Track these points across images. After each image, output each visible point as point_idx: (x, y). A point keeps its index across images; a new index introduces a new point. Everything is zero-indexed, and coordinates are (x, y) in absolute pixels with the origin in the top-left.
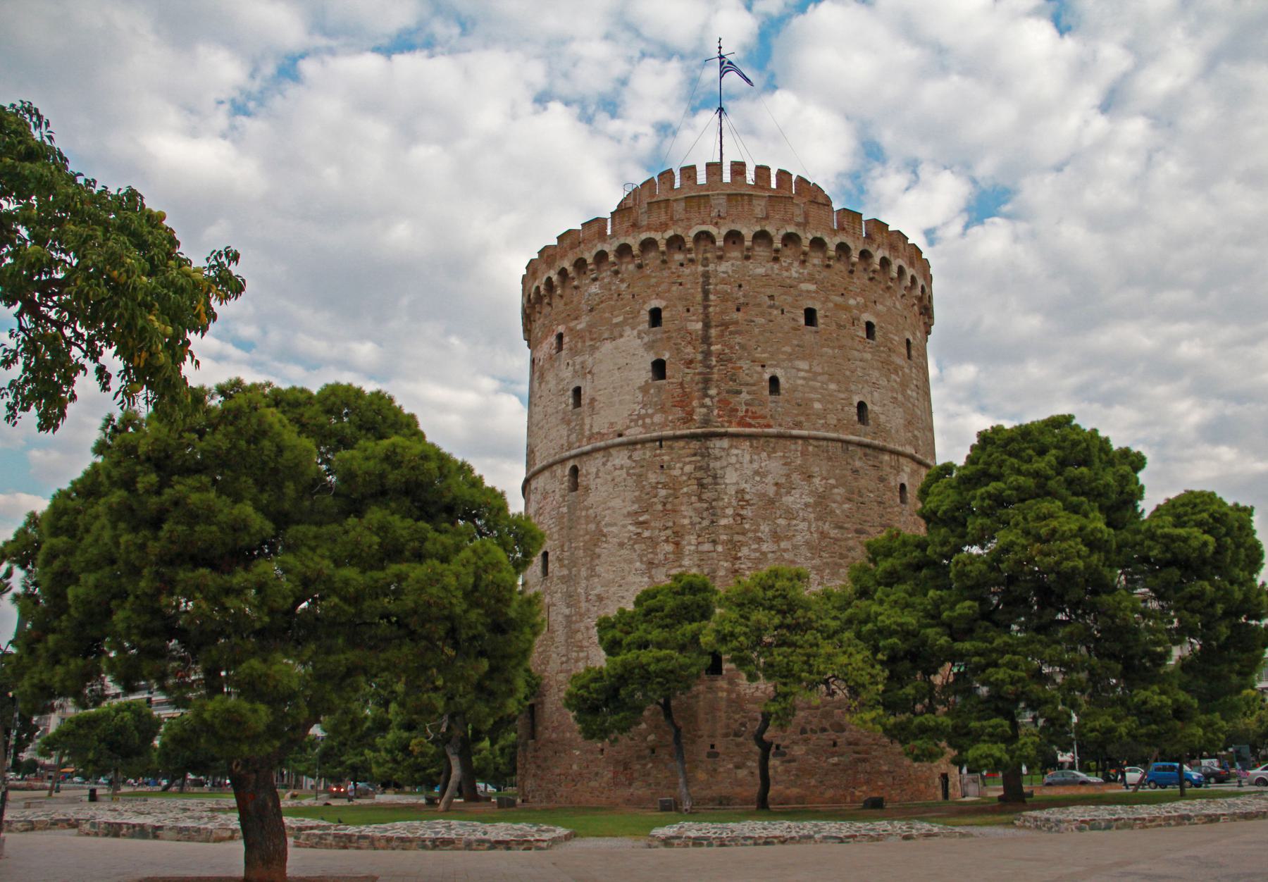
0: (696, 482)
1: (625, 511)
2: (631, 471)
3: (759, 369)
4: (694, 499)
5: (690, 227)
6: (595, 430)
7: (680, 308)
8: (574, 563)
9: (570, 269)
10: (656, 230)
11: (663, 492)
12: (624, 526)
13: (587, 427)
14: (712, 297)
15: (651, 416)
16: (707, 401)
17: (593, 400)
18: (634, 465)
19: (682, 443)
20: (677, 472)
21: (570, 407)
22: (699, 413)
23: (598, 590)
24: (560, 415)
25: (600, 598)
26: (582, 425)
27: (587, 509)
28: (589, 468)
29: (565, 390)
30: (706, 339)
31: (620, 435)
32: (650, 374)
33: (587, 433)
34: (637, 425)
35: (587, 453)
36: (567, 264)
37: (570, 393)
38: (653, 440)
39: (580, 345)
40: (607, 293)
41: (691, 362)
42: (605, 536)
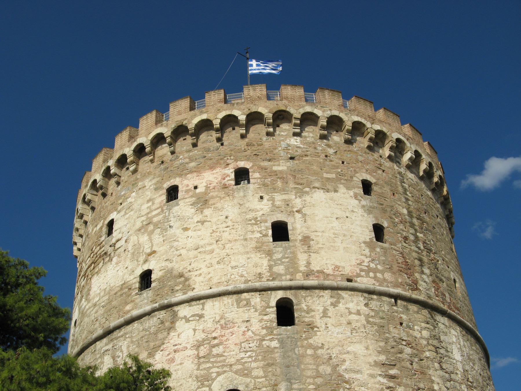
0: (433, 349)
1: (371, 360)
2: (371, 319)
3: (447, 268)
4: (437, 365)
6: (315, 267)
7: (387, 189)
10: (365, 119)
12: (372, 376)
14: (408, 193)
15: (382, 272)
16: (424, 277)
17: (306, 240)
18: (373, 314)
19: (413, 308)
20: (417, 334)
21: (271, 239)
22: (422, 286)
24: (253, 244)
27: (316, 348)
29: (256, 221)
30: (412, 225)
31: (349, 280)
32: (373, 235)
33: (302, 268)
34: (367, 276)
37: (269, 224)
38: (390, 296)
40: (311, 150)
41: (406, 238)
42: (347, 382)
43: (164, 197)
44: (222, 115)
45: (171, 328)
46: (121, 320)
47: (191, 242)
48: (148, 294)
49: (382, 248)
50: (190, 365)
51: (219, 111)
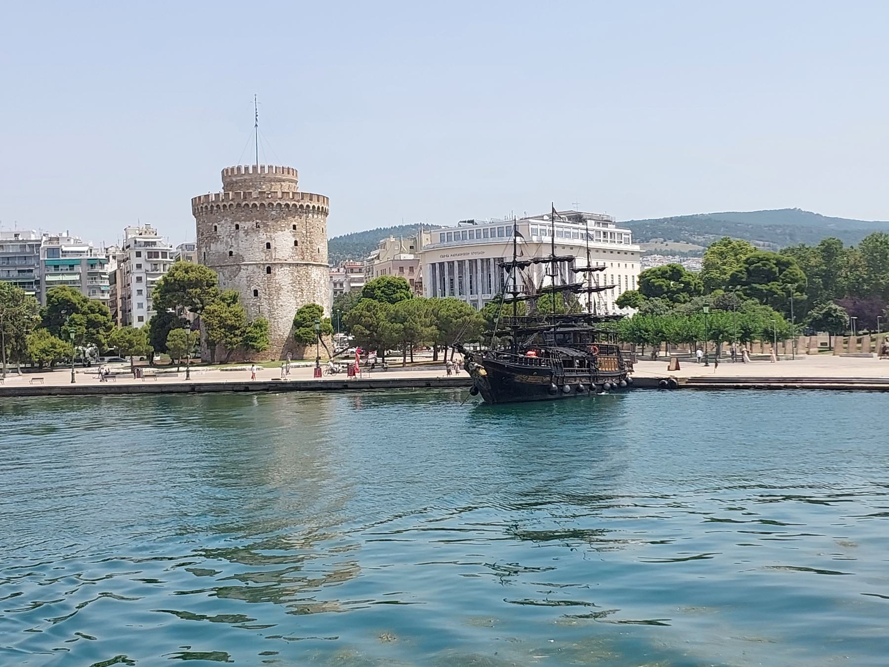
5: (305, 203)
8: (270, 295)
9: (266, 205)
11: (299, 278)
13: (274, 255)
17: (275, 248)
23: (281, 303)
25: (282, 306)
26: (271, 254)
27: (276, 280)
28: (276, 270)
30: (306, 236)
33: (274, 258)
35: (274, 264)
36: (264, 202)
37: (265, 243)
39: (269, 229)
41: (303, 242)
43: (235, 227)
44: (252, 203)
45: (240, 271)
46: (225, 264)
47: (244, 246)
48: (232, 259)
49: (296, 248)
50: (245, 282)
51: (251, 201)
